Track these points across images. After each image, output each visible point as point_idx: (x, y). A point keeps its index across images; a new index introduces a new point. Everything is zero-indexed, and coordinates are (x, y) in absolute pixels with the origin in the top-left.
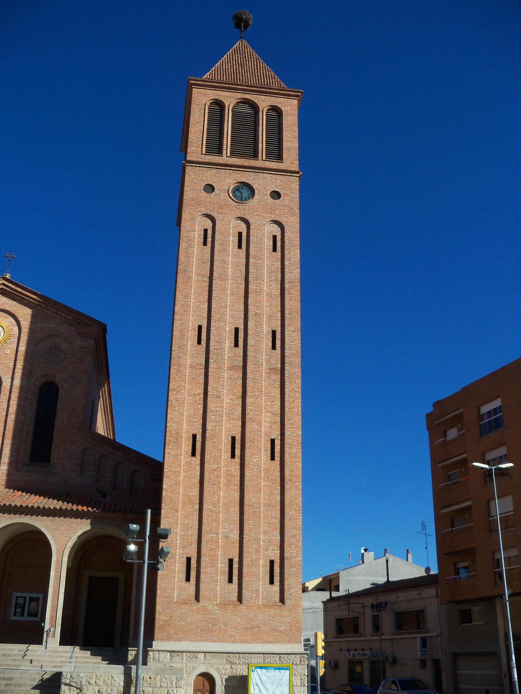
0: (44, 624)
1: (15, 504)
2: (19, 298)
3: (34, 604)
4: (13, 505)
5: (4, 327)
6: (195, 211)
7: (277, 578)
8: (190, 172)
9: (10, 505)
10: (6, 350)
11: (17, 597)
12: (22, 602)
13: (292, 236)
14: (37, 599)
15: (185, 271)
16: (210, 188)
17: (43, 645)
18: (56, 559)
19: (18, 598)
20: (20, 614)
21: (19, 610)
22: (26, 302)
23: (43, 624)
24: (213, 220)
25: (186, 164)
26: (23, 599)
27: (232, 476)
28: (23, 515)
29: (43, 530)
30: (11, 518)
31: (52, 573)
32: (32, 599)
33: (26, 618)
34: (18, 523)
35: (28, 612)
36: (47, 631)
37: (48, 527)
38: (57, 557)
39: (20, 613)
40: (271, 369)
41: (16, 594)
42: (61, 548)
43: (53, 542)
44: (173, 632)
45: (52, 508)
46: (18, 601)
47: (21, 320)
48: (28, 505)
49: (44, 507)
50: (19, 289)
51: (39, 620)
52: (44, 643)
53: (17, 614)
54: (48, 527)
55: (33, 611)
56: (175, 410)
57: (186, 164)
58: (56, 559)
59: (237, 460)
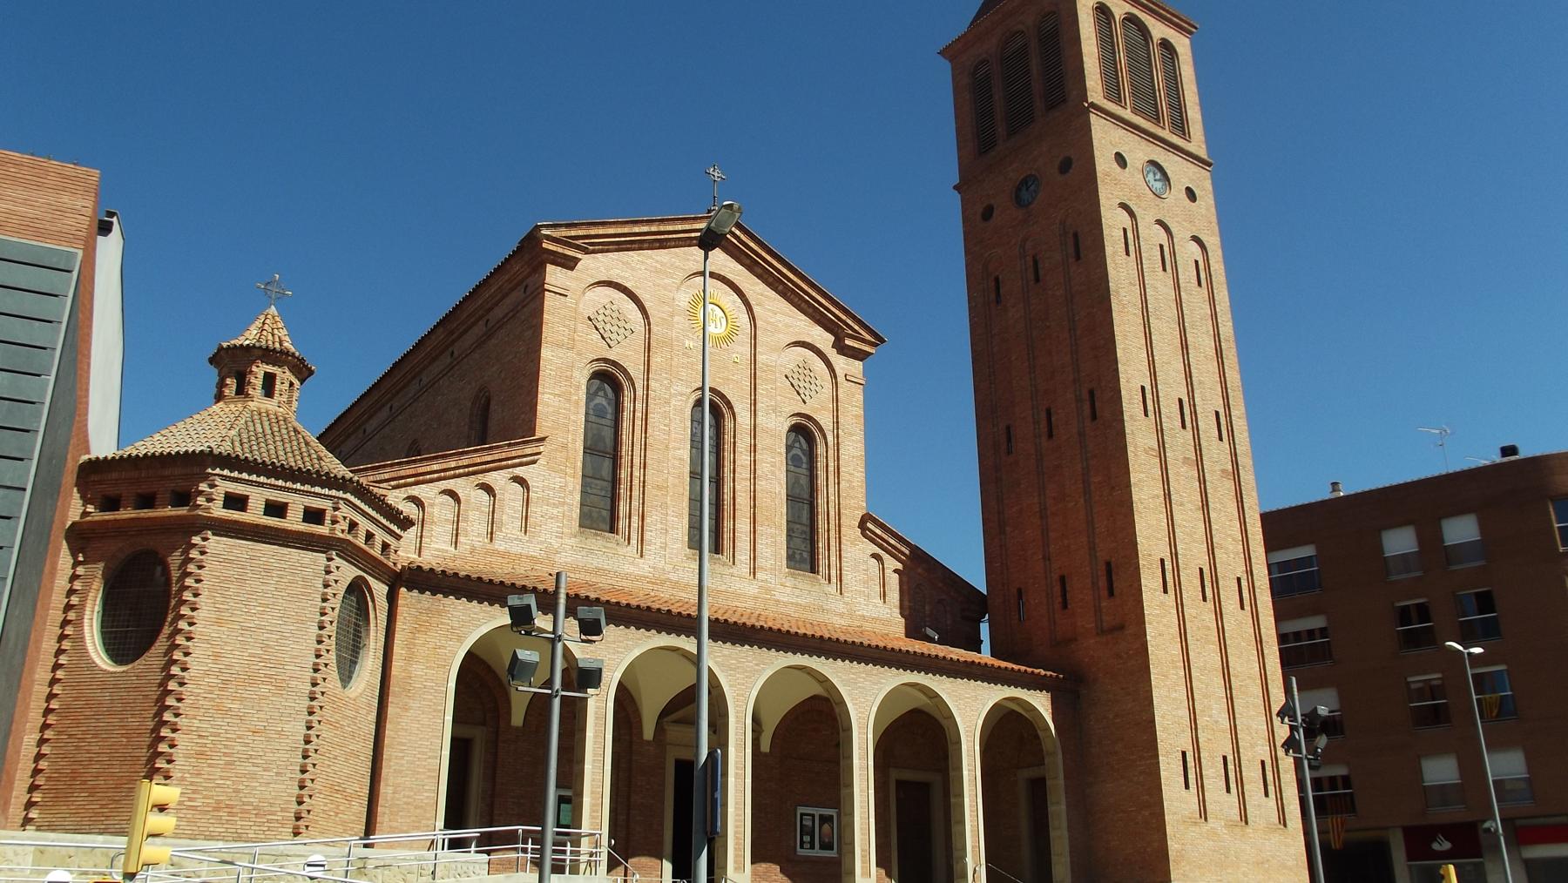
2: (748, 262)
3: (826, 827)
5: (726, 311)
6: (1112, 194)
7: (1271, 788)
8: (1098, 125)
10: (734, 355)
11: (802, 815)
13: (1217, 267)
15: (1118, 292)
16: (1121, 160)
21: (807, 838)
22: (759, 271)
24: (1132, 214)
25: (1091, 109)
27: (1209, 628)
31: (965, 773)
33: (817, 852)
35: (820, 841)
40: (1223, 471)
41: (801, 810)
44: (1188, 868)
46: (804, 823)
47: (752, 303)
50: (752, 245)
55: (827, 840)
56: (1141, 517)
57: (1091, 109)
59: (1210, 604)
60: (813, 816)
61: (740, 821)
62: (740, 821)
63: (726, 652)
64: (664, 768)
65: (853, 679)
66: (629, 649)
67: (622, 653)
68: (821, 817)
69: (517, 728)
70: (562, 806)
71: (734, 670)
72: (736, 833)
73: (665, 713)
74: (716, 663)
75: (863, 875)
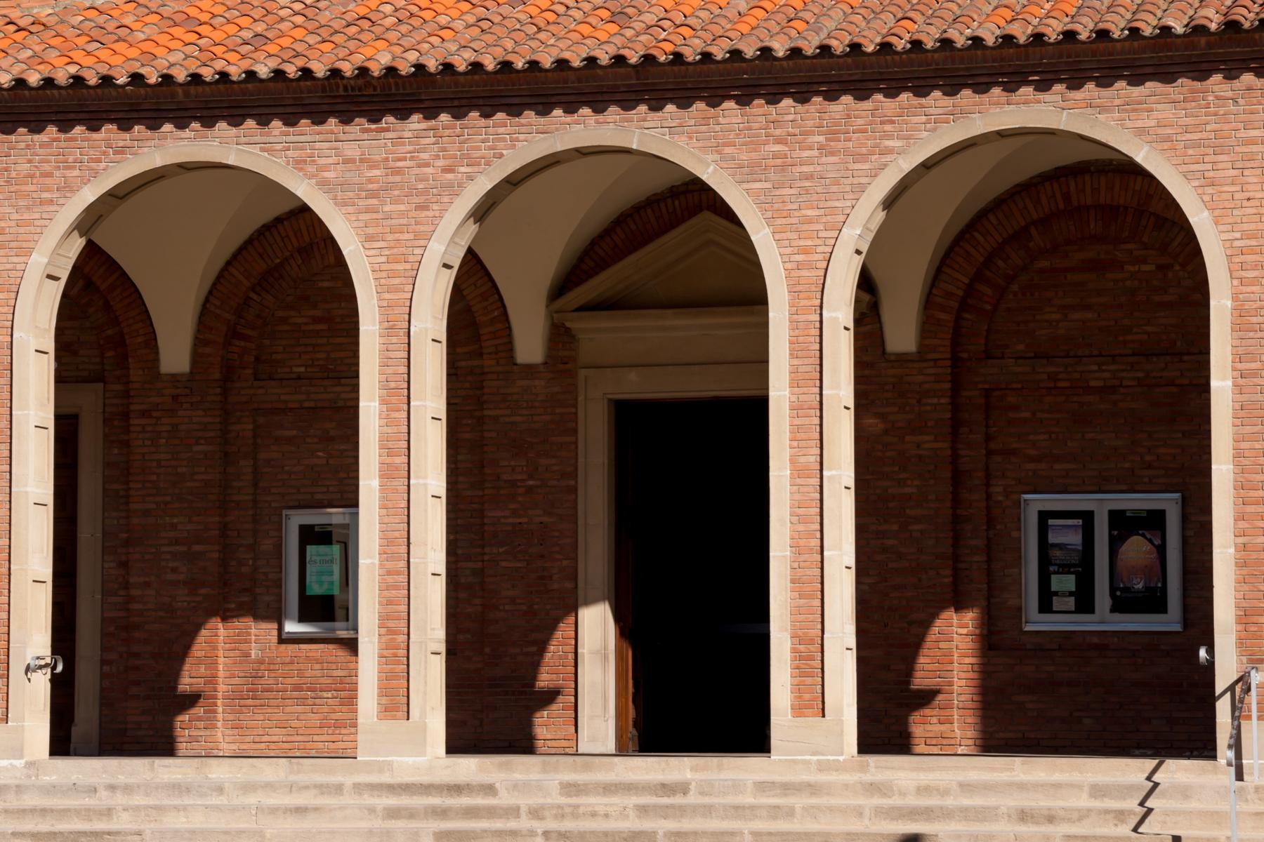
0: (1211, 651)
1: (968, 31)
3: (1136, 549)
4: (960, 41)
9: (946, 43)
11: (1044, 516)
12: (1075, 539)
14: (1155, 520)
17: (1222, 761)
18: (1229, 303)
19: (1051, 522)
20: (1071, 602)
21: (1064, 583)
23: (1203, 653)
26: (1080, 522)
28: (1026, 91)
29: (1142, 155)
30: (957, 114)
32: (1123, 524)
34: (1001, 134)
36: (1231, 688)
37: (1168, 139)
38: (1235, 298)
39: (1071, 594)
41: (1037, 502)
42: (1253, 242)
43: (1206, 213)
45: (1179, 29)
46: (1053, 538)
48: (1042, 29)
49: (1135, 32)
51: (1177, 628)
52: (1225, 753)
53: (1057, 603)
54: (1168, 139)
58: (1234, 309)
60: (1087, 517)
61: (396, 587)
62: (396, 587)
63: (351, 150)
64: (575, 431)
65: (776, 156)
66: (68, 189)
67: (51, 202)
68: (1116, 518)
69: (174, 378)
70: (311, 550)
71: (373, 195)
72: (384, 619)
73: (560, 289)
74: (323, 184)
75: (799, 709)
